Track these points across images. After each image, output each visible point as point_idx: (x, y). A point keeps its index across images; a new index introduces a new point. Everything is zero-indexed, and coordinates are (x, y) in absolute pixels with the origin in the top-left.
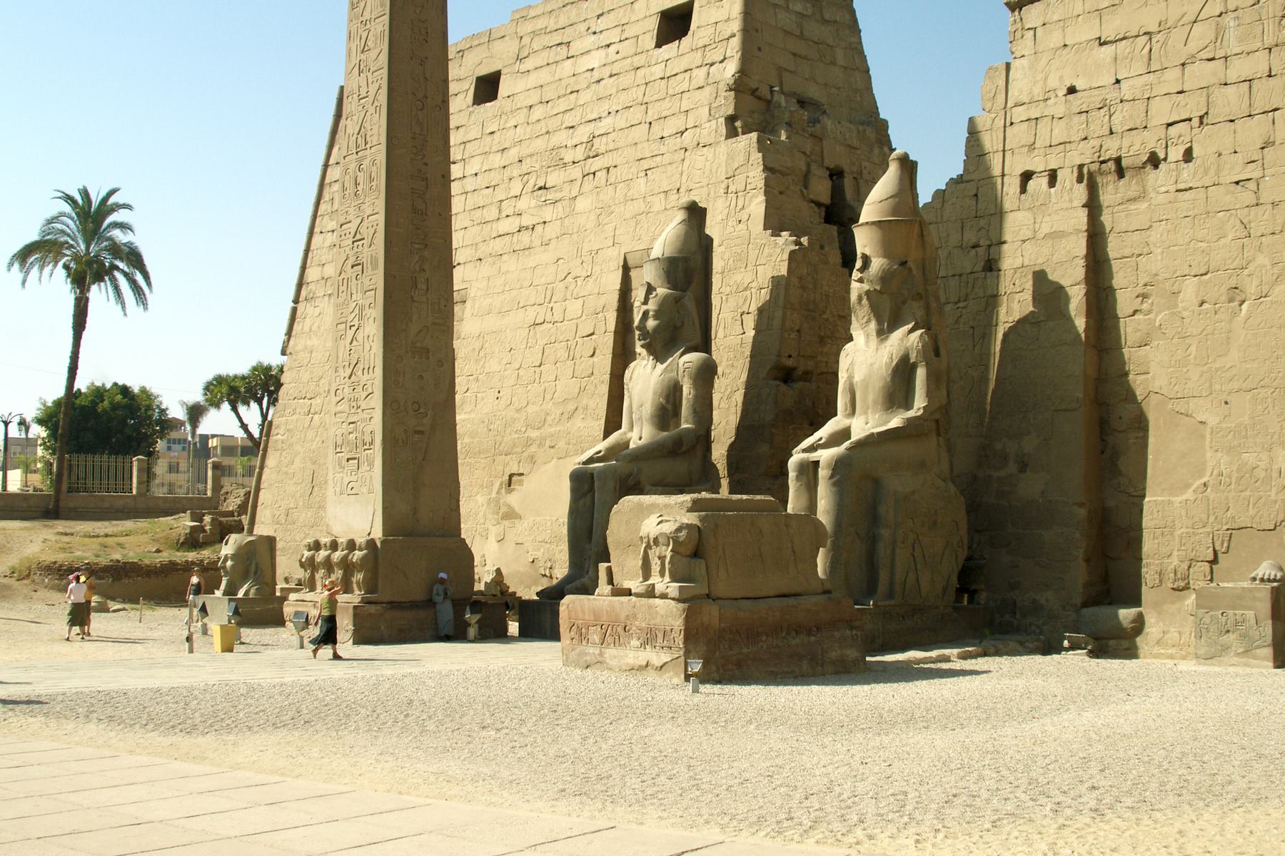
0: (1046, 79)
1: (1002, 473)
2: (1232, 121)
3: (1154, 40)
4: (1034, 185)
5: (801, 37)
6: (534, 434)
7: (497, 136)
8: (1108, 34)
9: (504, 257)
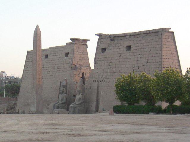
5: (80, 57)
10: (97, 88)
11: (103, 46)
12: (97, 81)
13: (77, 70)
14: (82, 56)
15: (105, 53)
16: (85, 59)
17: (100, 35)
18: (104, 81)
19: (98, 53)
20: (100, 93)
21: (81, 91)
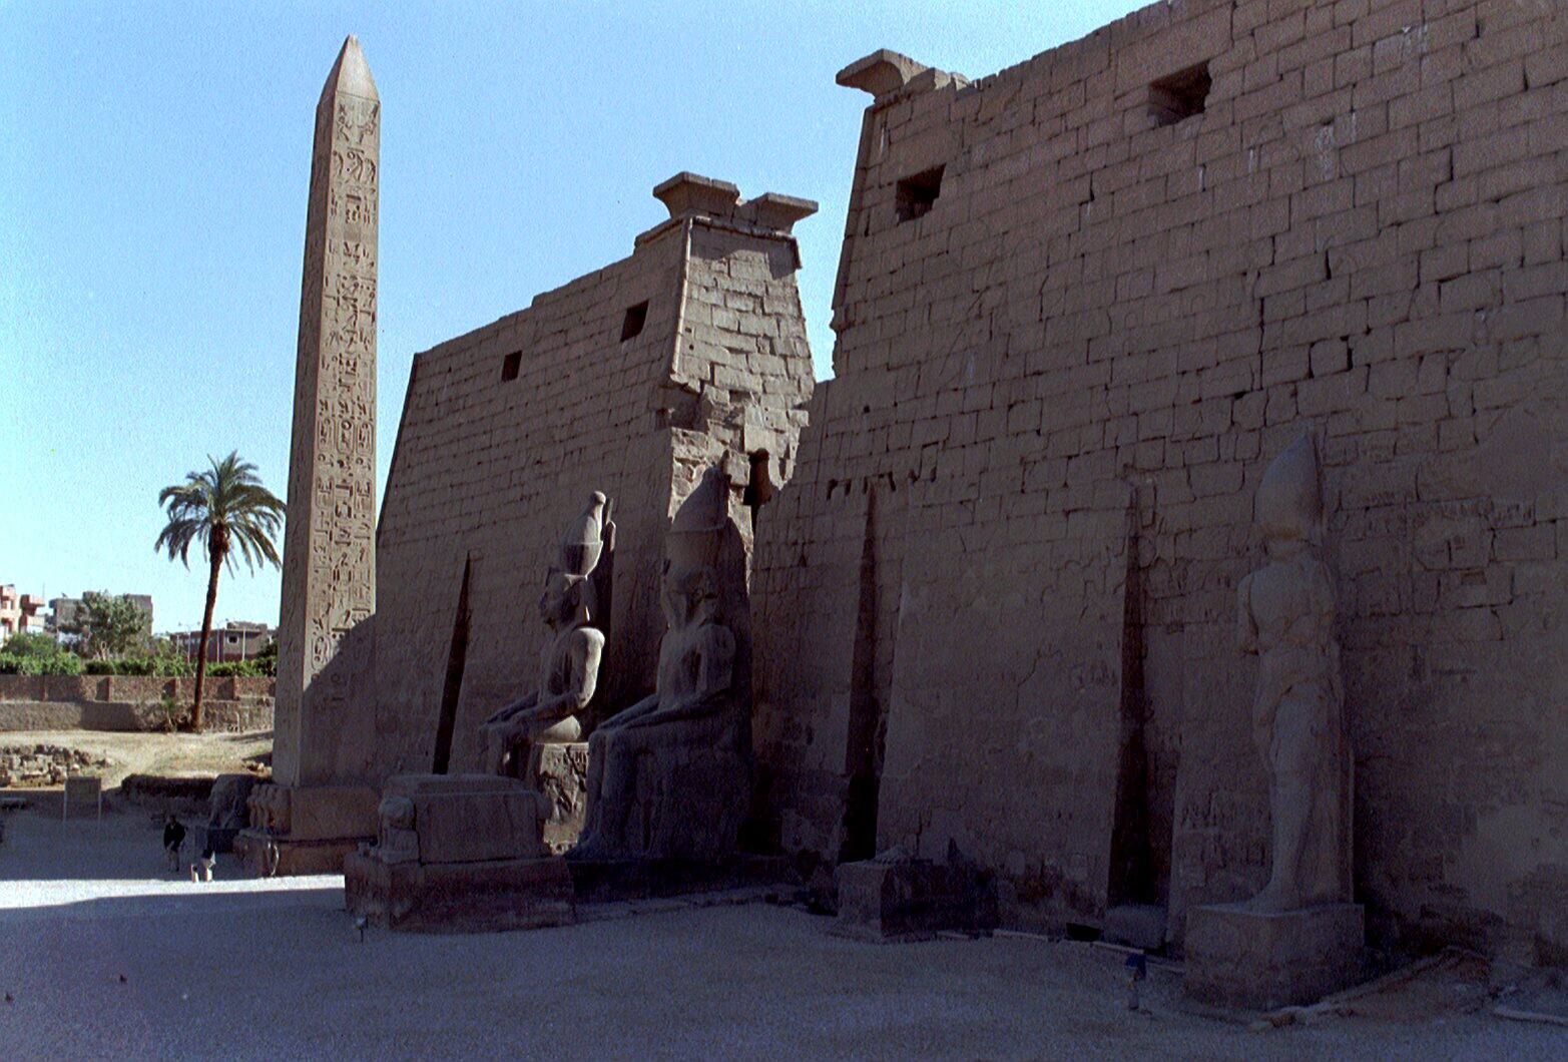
4: (839, 490)
6: (514, 680)
8: (894, 361)
10: (858, 547)
11: (909, 162)
12: (857, 486)
13: (706, 430)
14: (754, 324)
15: (929, 220)
16: (780, 348)
17: (871, 73)
18: (926, 473)
19: (866, 234)
20: (887, 600)
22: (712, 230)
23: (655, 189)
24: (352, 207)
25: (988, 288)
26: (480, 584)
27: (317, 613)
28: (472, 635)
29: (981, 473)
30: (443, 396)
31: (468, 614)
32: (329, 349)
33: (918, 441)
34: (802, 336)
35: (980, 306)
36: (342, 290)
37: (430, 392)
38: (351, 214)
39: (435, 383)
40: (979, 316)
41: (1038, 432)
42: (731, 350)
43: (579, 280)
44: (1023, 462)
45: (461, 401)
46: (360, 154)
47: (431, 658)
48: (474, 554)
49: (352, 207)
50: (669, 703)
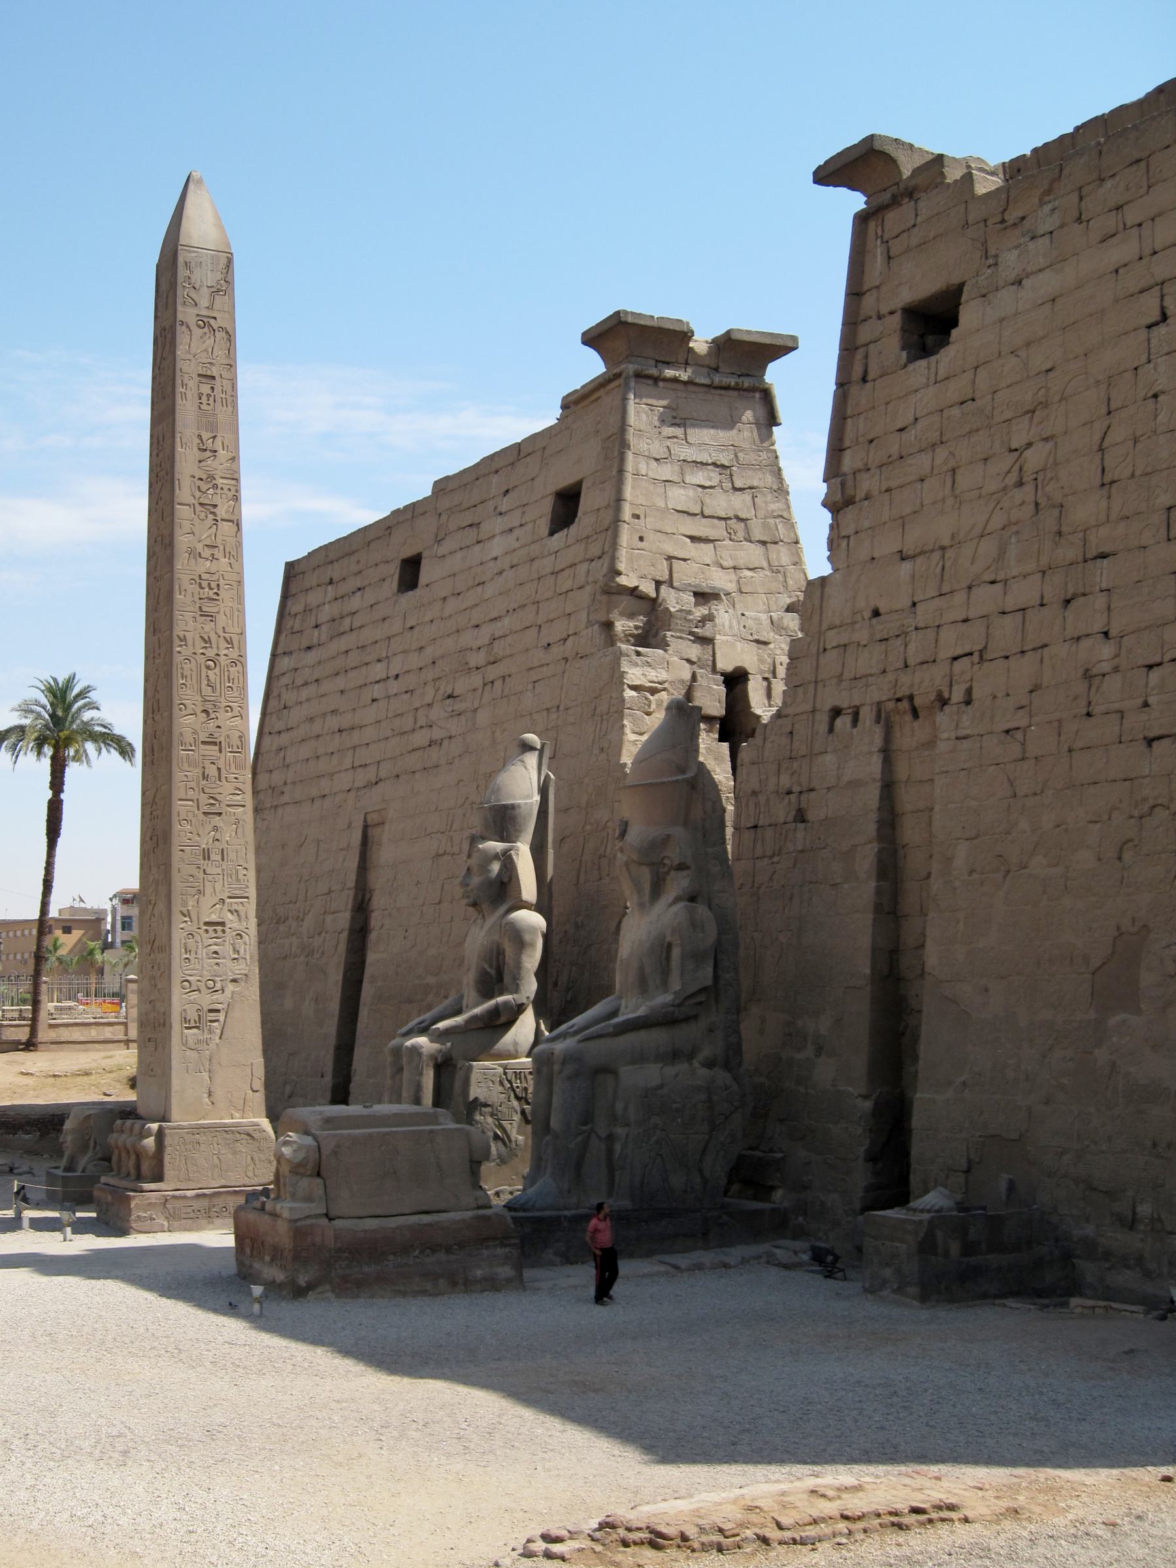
0: (855, 598)
1: (800, 1056)
2: (1007, 657)
3: (947, 555)
6: (431, 980)
7: (416, 630)
8: (909, 549)
9: (417, 775)
10: (872, 795)
11: (917, 283)
12: (867, 714)
13: (664, 645)
14: (721, 503)
15: (946, 358)
16: (757, 534)
18: (957, 695)
21: (674, 855)
22: (661, 384)
23: (583, 334)
24: (205, 389)
25: (1029, 445)
26: (386, 854)
27: (185, 904)
28: (375, 921)
29: (1031, 692)
30: (324, 616)
31: (367, 898)
32: (184, 569)
33: (945, 653)
34: (785, 515)
35: (1021, 469)
36: (198, 494)
37: (307, 610)
38: (204, 399)
39: (313, 598)
40: (1020, 484)
41: (1106, 634)
42: (693, 539)
43: (491, 458)
44: (1088, 675)
45: (347, 621)
46: (212, 322)
47: (323, 953)
48: (373, 818)
49: (205, 389)
50: (633, 1008)
